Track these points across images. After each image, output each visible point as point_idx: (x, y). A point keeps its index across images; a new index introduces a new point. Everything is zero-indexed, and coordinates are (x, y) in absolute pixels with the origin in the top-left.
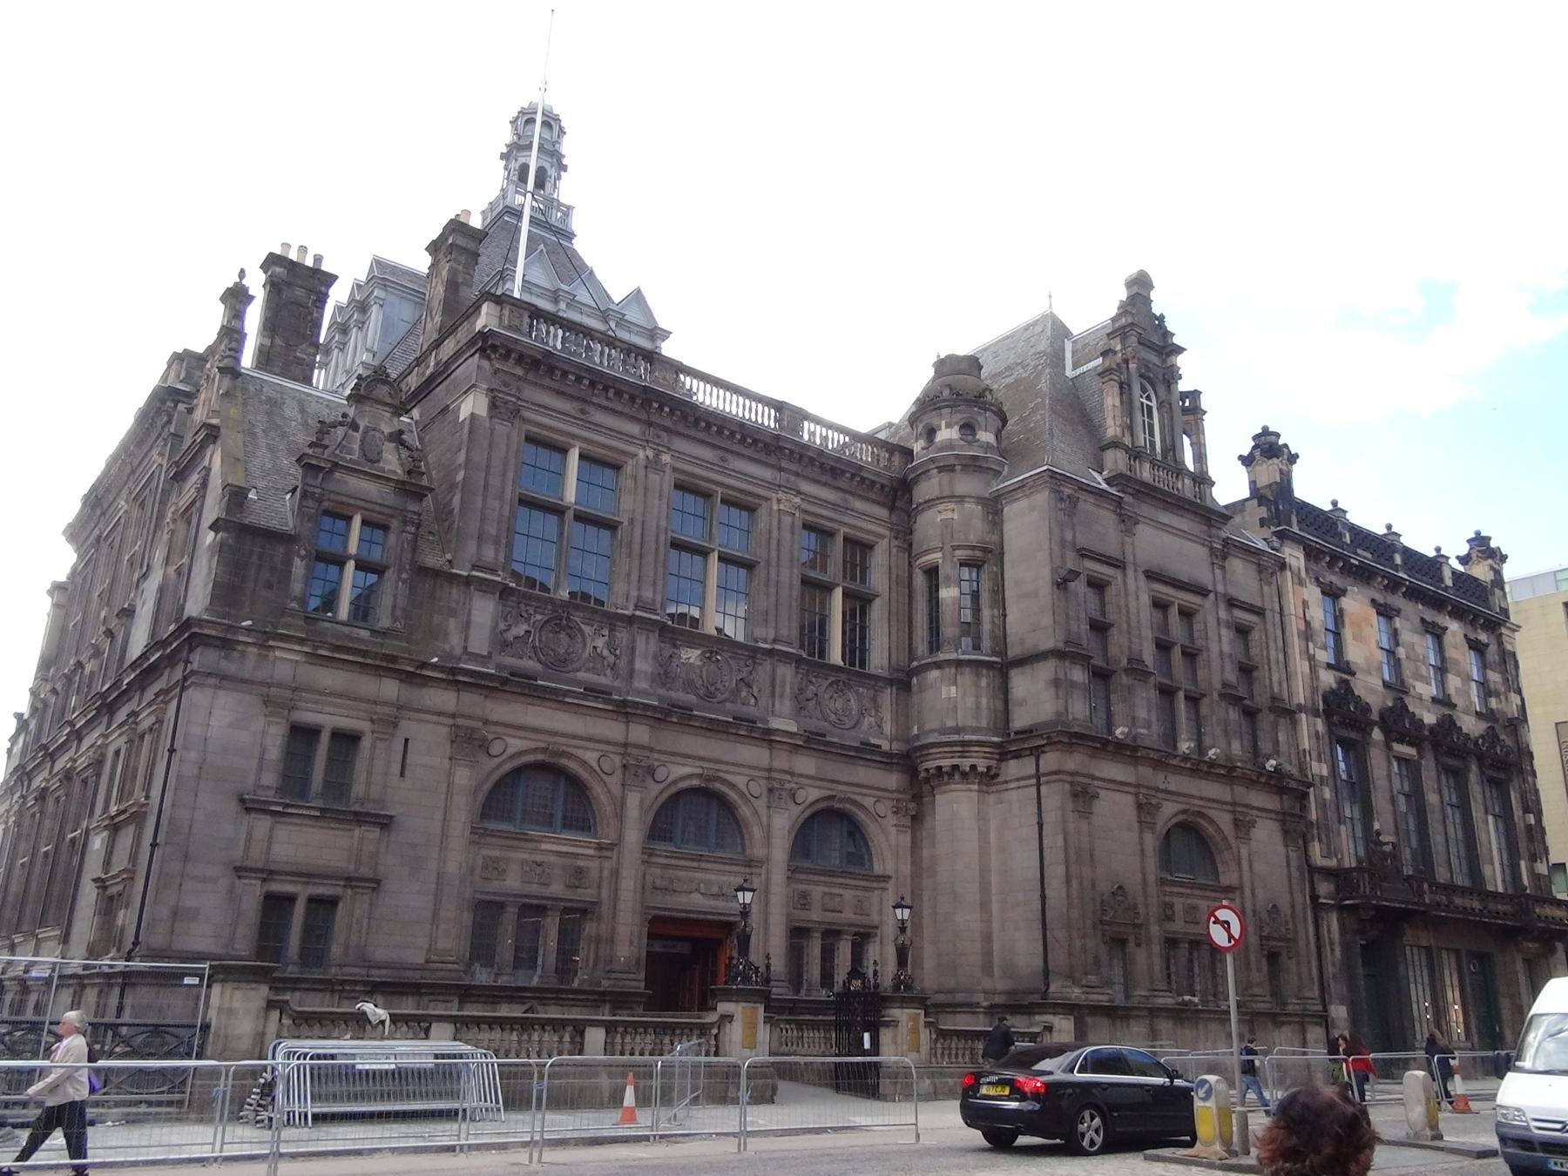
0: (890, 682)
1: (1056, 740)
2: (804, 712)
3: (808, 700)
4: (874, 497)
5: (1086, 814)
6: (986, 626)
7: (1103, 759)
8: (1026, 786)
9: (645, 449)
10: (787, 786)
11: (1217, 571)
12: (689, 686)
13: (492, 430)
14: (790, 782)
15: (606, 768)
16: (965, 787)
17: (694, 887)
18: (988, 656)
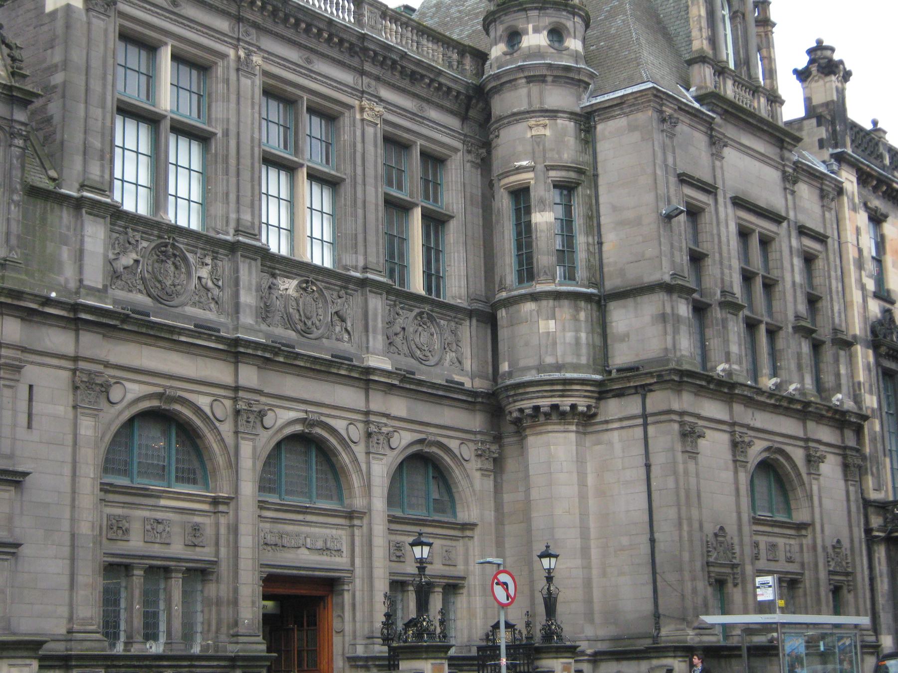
0: (471, 314)
1: (667, 378)
2: (392, 349)
3: (396, 334)
4: (447, 104)
5: (693, 454)
6: (581, 255)
7: (705, 397)
8: (630, 427)
9: (236, 48)
10: (385, 430)
11: (789, 197)
12: (288, 322)
13: (89, 23)
14: (386, 425)
15: (219, 414)
16: (561, 428)
17: (301, 542)
18: (581, 286)
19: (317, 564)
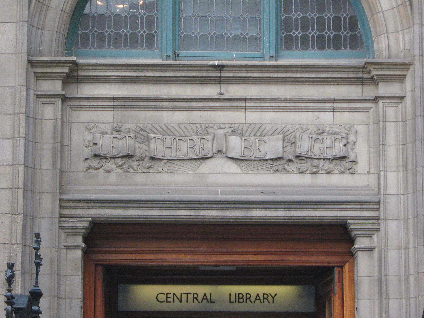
19: (262, 193)
